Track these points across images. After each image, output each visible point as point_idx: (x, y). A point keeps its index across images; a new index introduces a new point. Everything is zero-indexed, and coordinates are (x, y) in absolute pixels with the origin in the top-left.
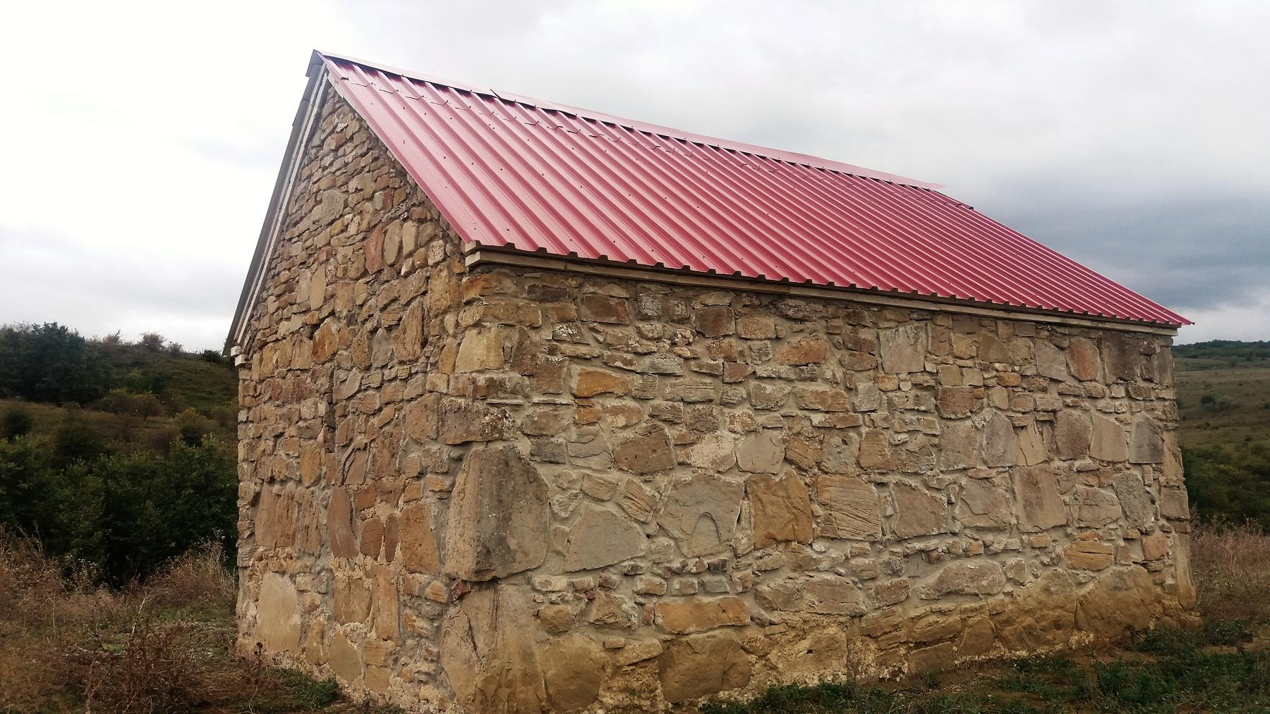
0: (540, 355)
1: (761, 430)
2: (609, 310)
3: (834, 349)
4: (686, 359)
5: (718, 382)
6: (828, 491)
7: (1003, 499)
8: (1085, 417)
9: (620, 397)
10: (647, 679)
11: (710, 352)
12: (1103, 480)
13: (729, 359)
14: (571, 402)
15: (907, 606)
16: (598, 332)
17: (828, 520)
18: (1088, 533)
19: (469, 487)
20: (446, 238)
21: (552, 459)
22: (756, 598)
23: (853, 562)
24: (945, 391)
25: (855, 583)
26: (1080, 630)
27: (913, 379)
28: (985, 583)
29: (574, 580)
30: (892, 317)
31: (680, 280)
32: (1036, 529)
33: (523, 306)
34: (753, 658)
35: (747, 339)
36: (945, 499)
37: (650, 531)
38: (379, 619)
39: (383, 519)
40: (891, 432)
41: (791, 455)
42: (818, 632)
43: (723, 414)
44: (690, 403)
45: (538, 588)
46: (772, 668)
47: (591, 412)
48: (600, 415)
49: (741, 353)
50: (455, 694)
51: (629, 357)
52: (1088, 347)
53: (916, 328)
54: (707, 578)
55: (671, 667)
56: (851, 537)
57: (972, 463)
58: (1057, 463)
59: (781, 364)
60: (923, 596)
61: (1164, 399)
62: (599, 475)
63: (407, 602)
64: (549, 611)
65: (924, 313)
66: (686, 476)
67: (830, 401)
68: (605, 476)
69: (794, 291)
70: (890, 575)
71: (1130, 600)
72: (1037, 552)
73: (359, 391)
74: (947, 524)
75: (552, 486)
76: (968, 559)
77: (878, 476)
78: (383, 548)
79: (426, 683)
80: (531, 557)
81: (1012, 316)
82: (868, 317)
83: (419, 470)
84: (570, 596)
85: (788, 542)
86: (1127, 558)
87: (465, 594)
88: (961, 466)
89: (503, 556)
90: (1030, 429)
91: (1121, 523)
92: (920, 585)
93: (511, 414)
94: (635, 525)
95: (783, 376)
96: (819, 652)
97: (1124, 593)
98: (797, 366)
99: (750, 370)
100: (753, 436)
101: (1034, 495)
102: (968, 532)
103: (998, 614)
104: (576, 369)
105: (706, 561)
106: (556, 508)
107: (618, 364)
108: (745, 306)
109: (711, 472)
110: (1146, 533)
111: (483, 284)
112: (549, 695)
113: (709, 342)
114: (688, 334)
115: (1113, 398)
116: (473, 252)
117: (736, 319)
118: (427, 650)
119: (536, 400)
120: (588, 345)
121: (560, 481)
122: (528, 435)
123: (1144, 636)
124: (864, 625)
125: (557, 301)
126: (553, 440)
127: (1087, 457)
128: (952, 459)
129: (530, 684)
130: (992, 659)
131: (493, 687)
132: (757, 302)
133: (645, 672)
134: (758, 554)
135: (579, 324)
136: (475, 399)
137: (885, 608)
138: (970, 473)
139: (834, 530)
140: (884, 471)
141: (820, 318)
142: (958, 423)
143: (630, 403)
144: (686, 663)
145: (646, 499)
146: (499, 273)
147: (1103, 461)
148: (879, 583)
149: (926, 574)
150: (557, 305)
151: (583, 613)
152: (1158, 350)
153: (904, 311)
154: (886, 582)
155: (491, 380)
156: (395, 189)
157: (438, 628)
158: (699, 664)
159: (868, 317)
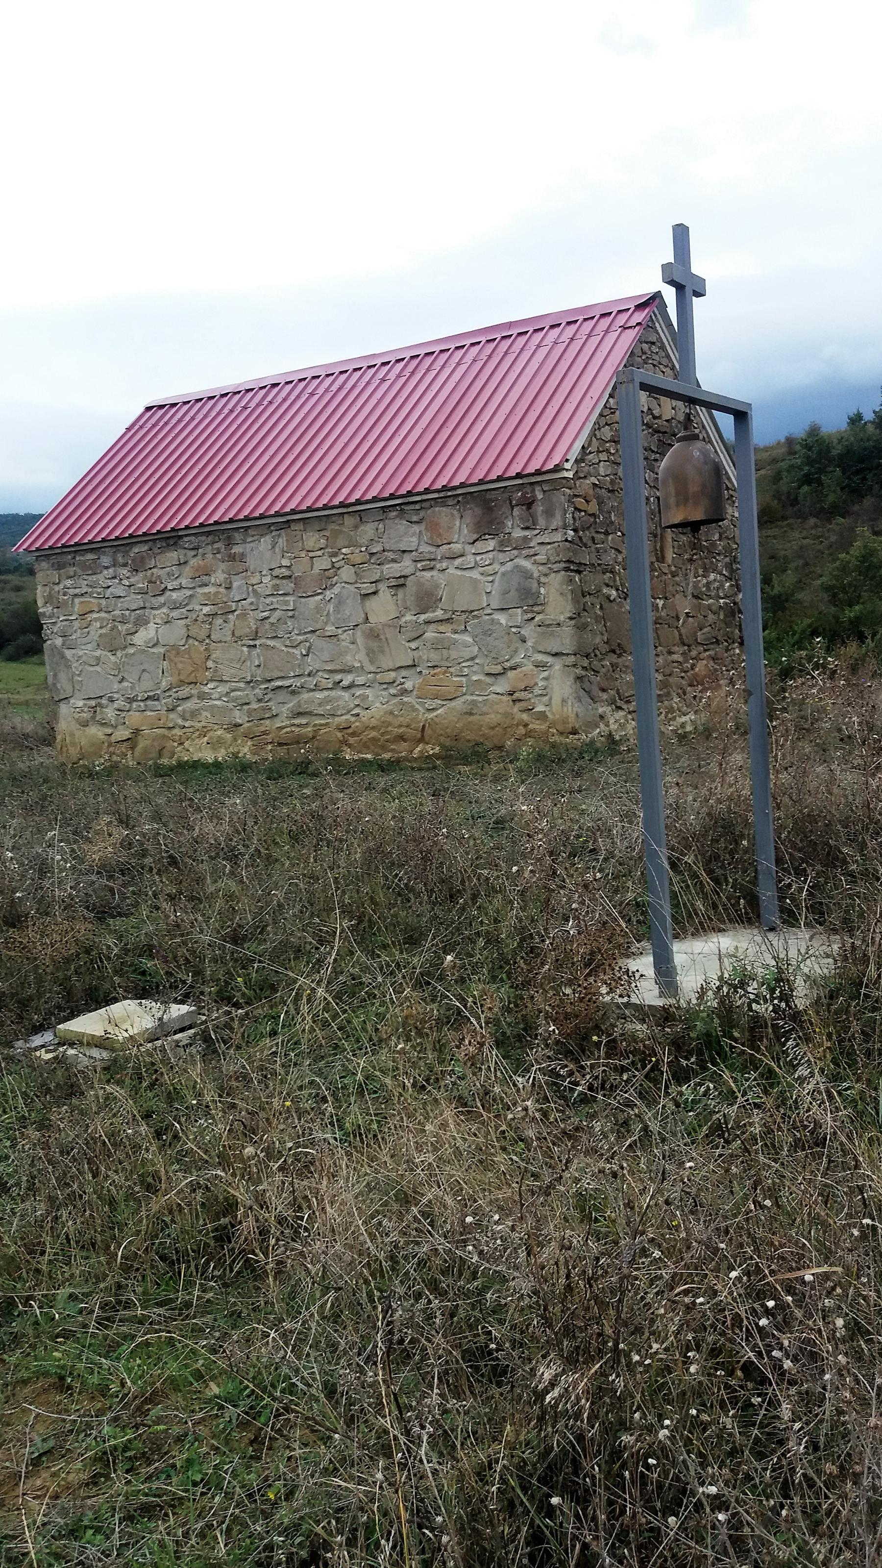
24: (296, 578)
30: (255, 533)
34: (176, 744)
51: (99, 590)
54: (149, 703)
66: (131, 650)
67: (212, 598)
82: (238, 536)
100: (168, 625)
101: (376, 644)
104: (77, 600)
107: (95, 595)
128: (303, 625)
149: (291, 701)
153: (263, 527)
159: (238, 536)
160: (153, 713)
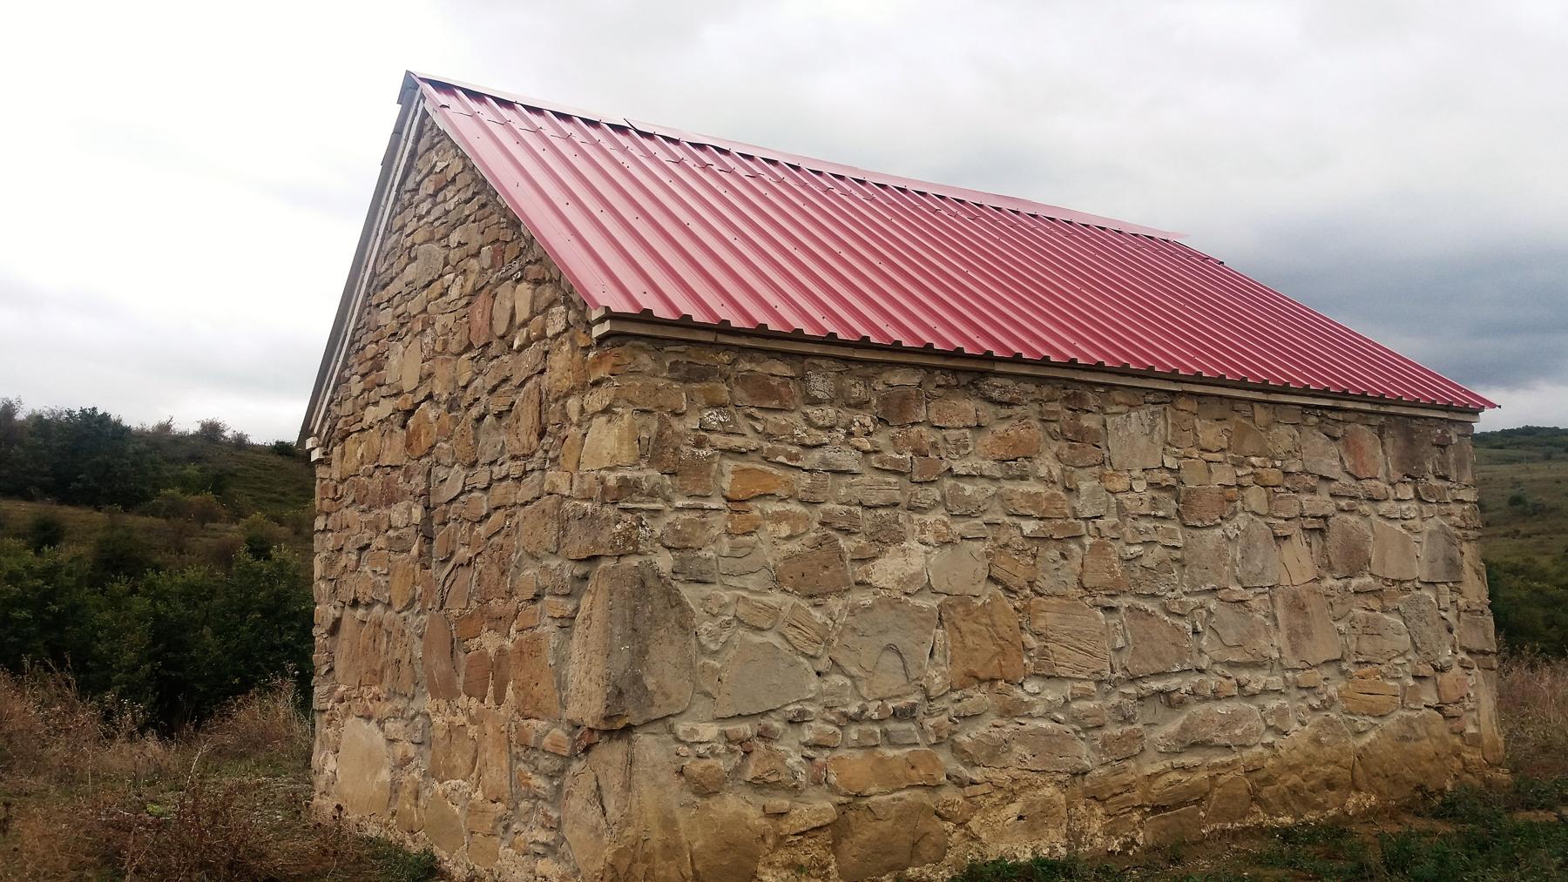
0: (684, 448)
1: (959, 541)
2: (771, 393)
3: (1049, 440)
4: (865, 453)
5: (905, 481)
6: (1044, 617)
7: (1263, 629)
8: (1363, 525)
9: (782, 500)
10: (817, 852)
11: (895, 444)
12: (1387, 603)
13: (918, 452)
14: (722, 506)
15: (1141, 761)
16: (756, 419)
17: (1043, 654)
18: (1368, 669)
19: (597, 613)
20: (568, 302)
21: (699, 578)
22: (953, 751)
23: (1075, 706)
24: (1188, 492)
25: (1077, 732)
26: (1358, 790)
27: (1148, 477)
28: (1238, 732)
29: (727, 728)
30: (1123, 400)
31: (858, 355)
32: (1304, 665)
33: (663, 388)
34: (949, 826)
35: (941, 428)
36: (1189, 627)
37: (820, 668)
38: (486, 777)
39: (491, 651)
40: (1121, 543)
41: (996, 572)
42: (1031, 793)
43: (911, 520)
44: (870, 507)
45: (682, 738)
46: (973, 839)
47: (747, 519)
48: (758, 523)
49: (934, 445)
50: (579, 870)
51: (794, 450)
52: (1366, 436)
53: (1153, 413)
54: (892, 726)
55: (847, 837)
56: (1072, 675)
57: (1222, 582)
58: (1329, 582)
59: (984, 459)
60: (1162, 749)
61: (1463, 502)
62: (757, 598)
63: (521, 754)
64: (695, 767)
65: (1163, 394)
66: (866, 599)
68: (765, 599)
69: (999, 368)
70: (1120, 722)
71: (1421, 753)
72: (1305, 693)
73: (462, 493)
74: (1191, 658)
75: (699, 611)
76: (1218, 703)
77: (1106, 599)
78: (490, 688)
79: (544, 856)
80: (673, 699)
81: (1272, 398)
82: (1092, 400)
83: (535, 591)
84: (721, 748)
85: (993, 680)
86: (1418, 700)
87: (593, 745)
88: (1210, 586)
89: (638, 699)
90: (1295, 539)
91: (1410, 657)
92: (1157, 734)
93: (648, 521)
94: (802, 659)
95: (986, 473)
96: (1032, 819)
97: (1413, 743)
98: (1004, 461)
99: (945, 465)
100: (948, 549)
101: (1300, 621)
102: (1218, 668)
103: (1255, 770)
104: (729, 465)
105: (891, 705)
106: (704, 639)
107: (781, 459)
108: (938, 386)
109: (898, 594)
110: (1441, 670)
111: (613, 360)
112: (694, 871)
113: (894, 431)
114: (868, 421)
115: (1399, 500)
116: (601, 320)
117: (927, 403)
118: (545, 815)
119: (679, 504)
120: (744, 435)
121: (710, 605)
122: (669, 548)
123: (1439, 798)
124: (1087, 784)
125: (706, 380)
126: (700, 553)
127: (1367, 574)
128: (1198, 578)
129: (672, 858)
130: (1248, 828)
131: (626, 861)
132: (953, 382)
133: (816, 843)
134: (956, 696)
135: (733, 410)
136: (604, 503)
137: (1114, 763)
138: (1221, 594)
139: (1051, 667)
140: (1113, 592)
141: (1032, 401)
142: (1205, 531)
143: (798, 508)
144: (866, 832)
145: (816, 627)
146: (634, 347)
147: (1387, 579)
148: (1106, 732)
150: (706, 386)
151: (738, 770)
152: (1455, 440)
154: (1115, 731)
155: (624, 479)
156: (507, 243)
157: (559, 787)
158: (883, 833)
159: (1092, 400)
160: (896, 752)
